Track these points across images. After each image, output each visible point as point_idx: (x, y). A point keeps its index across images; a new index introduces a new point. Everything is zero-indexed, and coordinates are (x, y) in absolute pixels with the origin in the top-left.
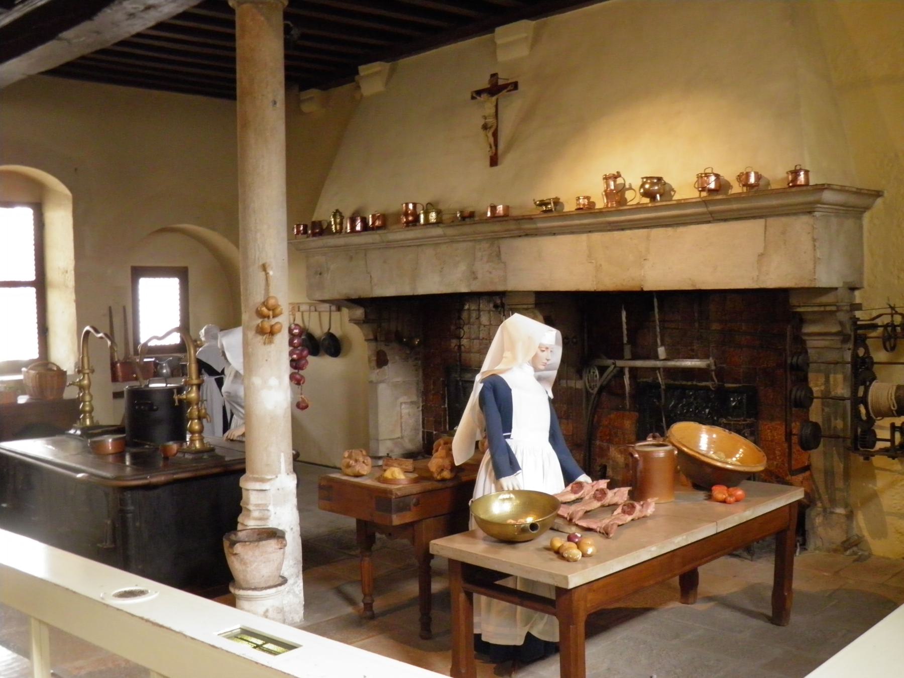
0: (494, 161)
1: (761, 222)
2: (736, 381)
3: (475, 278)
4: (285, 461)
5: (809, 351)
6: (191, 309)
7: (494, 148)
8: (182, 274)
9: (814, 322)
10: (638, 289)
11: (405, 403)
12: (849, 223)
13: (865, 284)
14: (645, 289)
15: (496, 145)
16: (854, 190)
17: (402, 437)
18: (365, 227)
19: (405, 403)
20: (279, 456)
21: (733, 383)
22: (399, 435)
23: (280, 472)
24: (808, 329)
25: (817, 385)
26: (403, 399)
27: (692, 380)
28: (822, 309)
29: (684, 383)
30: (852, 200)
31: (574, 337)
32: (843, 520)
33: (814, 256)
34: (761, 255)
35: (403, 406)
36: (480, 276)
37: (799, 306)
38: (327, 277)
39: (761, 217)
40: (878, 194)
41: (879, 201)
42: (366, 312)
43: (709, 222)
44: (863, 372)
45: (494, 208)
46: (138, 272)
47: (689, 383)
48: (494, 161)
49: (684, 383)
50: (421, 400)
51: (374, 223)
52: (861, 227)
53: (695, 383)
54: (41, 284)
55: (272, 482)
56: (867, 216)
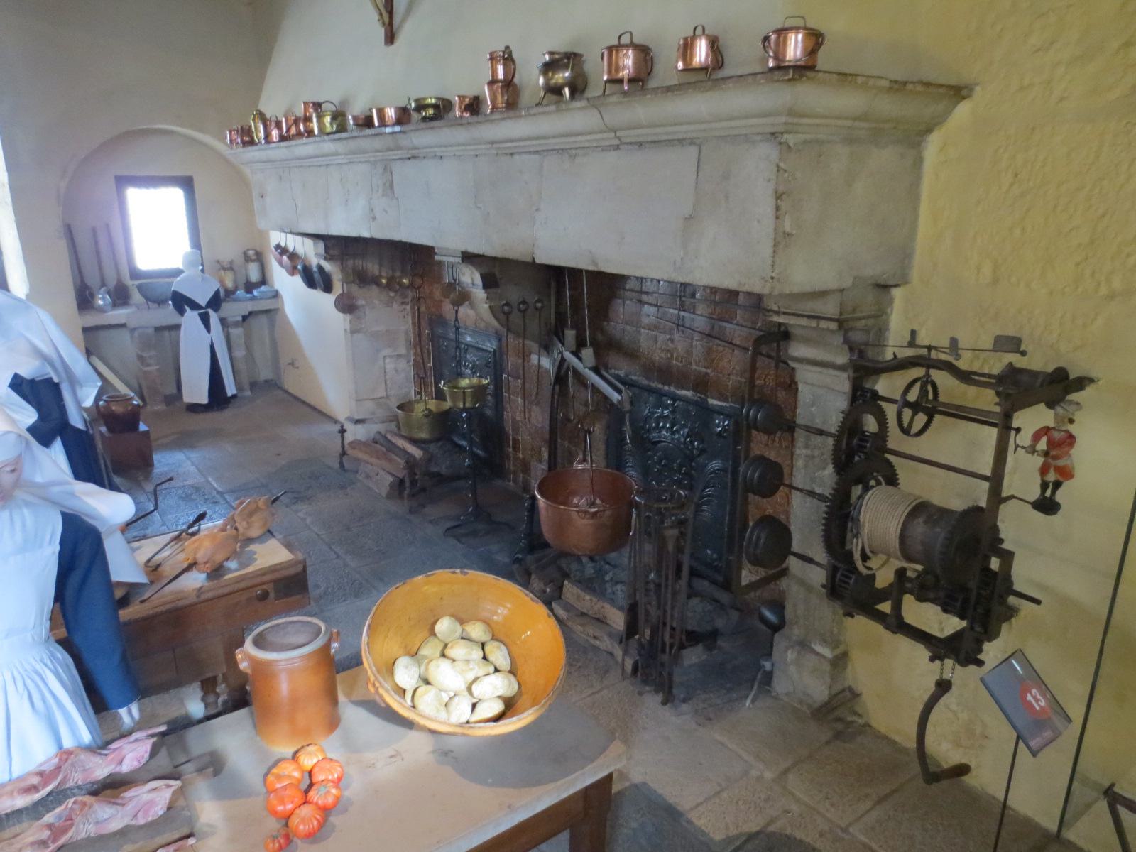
0: (390, 38)
1: (693, 151)
2: (722, 397)
3: (374, 219)
5: (800, 387)
6: (201, 226)
7: (386, 16)
8: (187, 183)
9: (807, 341)
10: (529, 259)
11: (391, 357)
12: (885, 157)
13: (915, 275)
14: (538, 261)
15: (391, 13)
17: (387, 397)
18: (283, 138)
21: (719, 400)
22: (383, 394)
24: (798, 350)
25: (807, 447)
26: (387, 352)
27: (669, 385)
29: (660, 386)
30: (887, 106)
31: (539, 301)
32: (827, 667)
33: (775, 229)
34: (689, 219)
35: (388, 360)
36: (378, 215)
37: (777, 313)
39: (692, 142)
40: (959, 92)
41: (963, 110)
43: (617, 147)
44: (861, 458)
45: (381, 113)
46: (123, 181)
47: (666, 388)
48: (390, 38)
49: (660, 386)
50: (412, 352)
51: (288, 130)
52: (918, 162)
53: (672, 389)
56: (934, 142)
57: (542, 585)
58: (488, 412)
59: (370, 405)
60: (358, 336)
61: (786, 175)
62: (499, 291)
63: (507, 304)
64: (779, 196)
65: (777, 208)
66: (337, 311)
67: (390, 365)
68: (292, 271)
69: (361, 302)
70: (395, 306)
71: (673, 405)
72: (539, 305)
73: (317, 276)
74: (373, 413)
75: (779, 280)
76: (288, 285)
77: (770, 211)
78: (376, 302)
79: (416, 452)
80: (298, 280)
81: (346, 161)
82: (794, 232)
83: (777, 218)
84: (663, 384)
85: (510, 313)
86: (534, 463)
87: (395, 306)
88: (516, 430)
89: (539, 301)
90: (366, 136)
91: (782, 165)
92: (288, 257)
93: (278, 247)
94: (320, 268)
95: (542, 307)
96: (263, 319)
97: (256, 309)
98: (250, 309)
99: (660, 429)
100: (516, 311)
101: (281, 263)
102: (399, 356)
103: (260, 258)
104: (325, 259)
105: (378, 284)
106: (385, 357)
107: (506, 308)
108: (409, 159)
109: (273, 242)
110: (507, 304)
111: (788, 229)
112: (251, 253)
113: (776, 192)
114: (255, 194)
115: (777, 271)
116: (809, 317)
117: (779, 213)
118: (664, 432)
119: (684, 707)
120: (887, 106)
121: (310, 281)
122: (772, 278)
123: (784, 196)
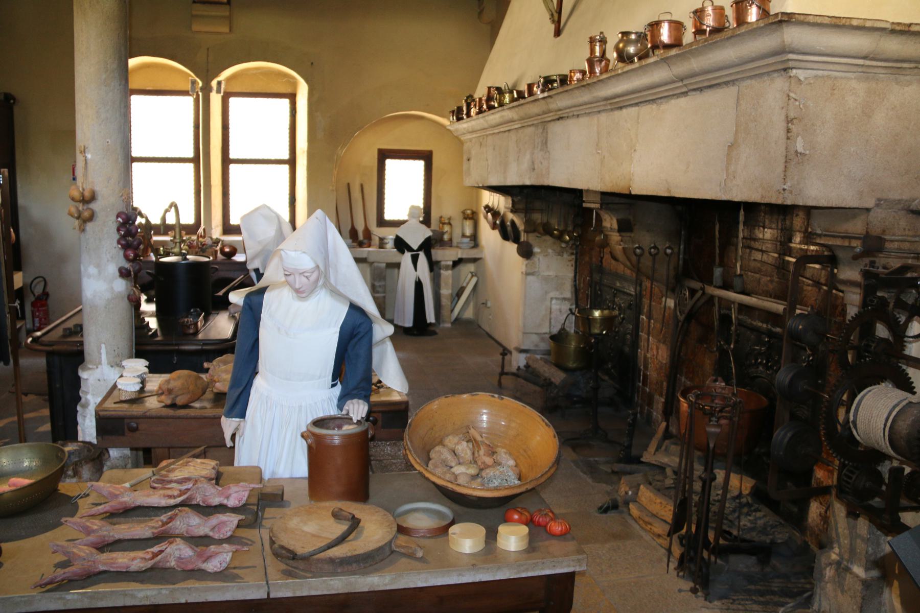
3: (534, 169)
4: (107, 353)
10: (627, 192)
11: (557, 299)
14: (633, 193)
16: (888, 26)
19: (557, 299)
20: (100, 349)
23: (100, 363)
28: (847, 244)
29: (760, 324)
30: (894, 46)
32: (859, 587)
35: (554, 302)
38: (472, 162)
42: (513, 201)
46: (384, 155)
49: (760, 324)
54: (292, 162)
55: (90, 372)
57: (627, 489)
58: (627, 349)
59: (535, 338)
60: (530, 278)
61: (797, 103)
62: (632, 235)
63: (639, 248)
64: (789, 121)
65: (788, 131)
66: (517, 255)
67: (555, 306)
68: (494, 227)
69: (536, 250)
70: (565, 256)
71: (769, 341)
72: (669, 251)
73: (509, 229)
74: (536, 346)
75: (791, 192)
76: (489, 236)
77: (782, 133)
78: (550, 251)
79: (558, 377)
80: (496, 234)
81: (519, 126)
82: (808, 152)
83: (788, 138)
84: (762, 322)
85: (641, 255)
86: (657, 397)
87: (565, 256)
88: (646, 367)
89: (669, 248)
90: (528, 103)
91: (792, 95)
92: (493, 215)
93: (487, 207)
94: (513, 222)
95: (671, 254)
96: (471, 267)
97: (464, 256)
98: (460, 256)
99: (757, 365)
100: (647, 254)
101: (486, 218)
102: (564, 299)
103: (473, 217)
104: (512, 211)
105: (552, 235)
106: (552, 299)
107: (638, 251)
108: (558, 119)
109: (484, 203)
110: (639, 248)
111: (800, 150)
112: (469, 212)
113: (787, 117)
114: (465, 158)
115: (789, 184)
116: (843, 237)
117: (789, 135)
118: (761, 368)
119: (717, 603)
120: (894, 46)
121: (505, 236)
122: (784, 190)
123: (795, 121)
